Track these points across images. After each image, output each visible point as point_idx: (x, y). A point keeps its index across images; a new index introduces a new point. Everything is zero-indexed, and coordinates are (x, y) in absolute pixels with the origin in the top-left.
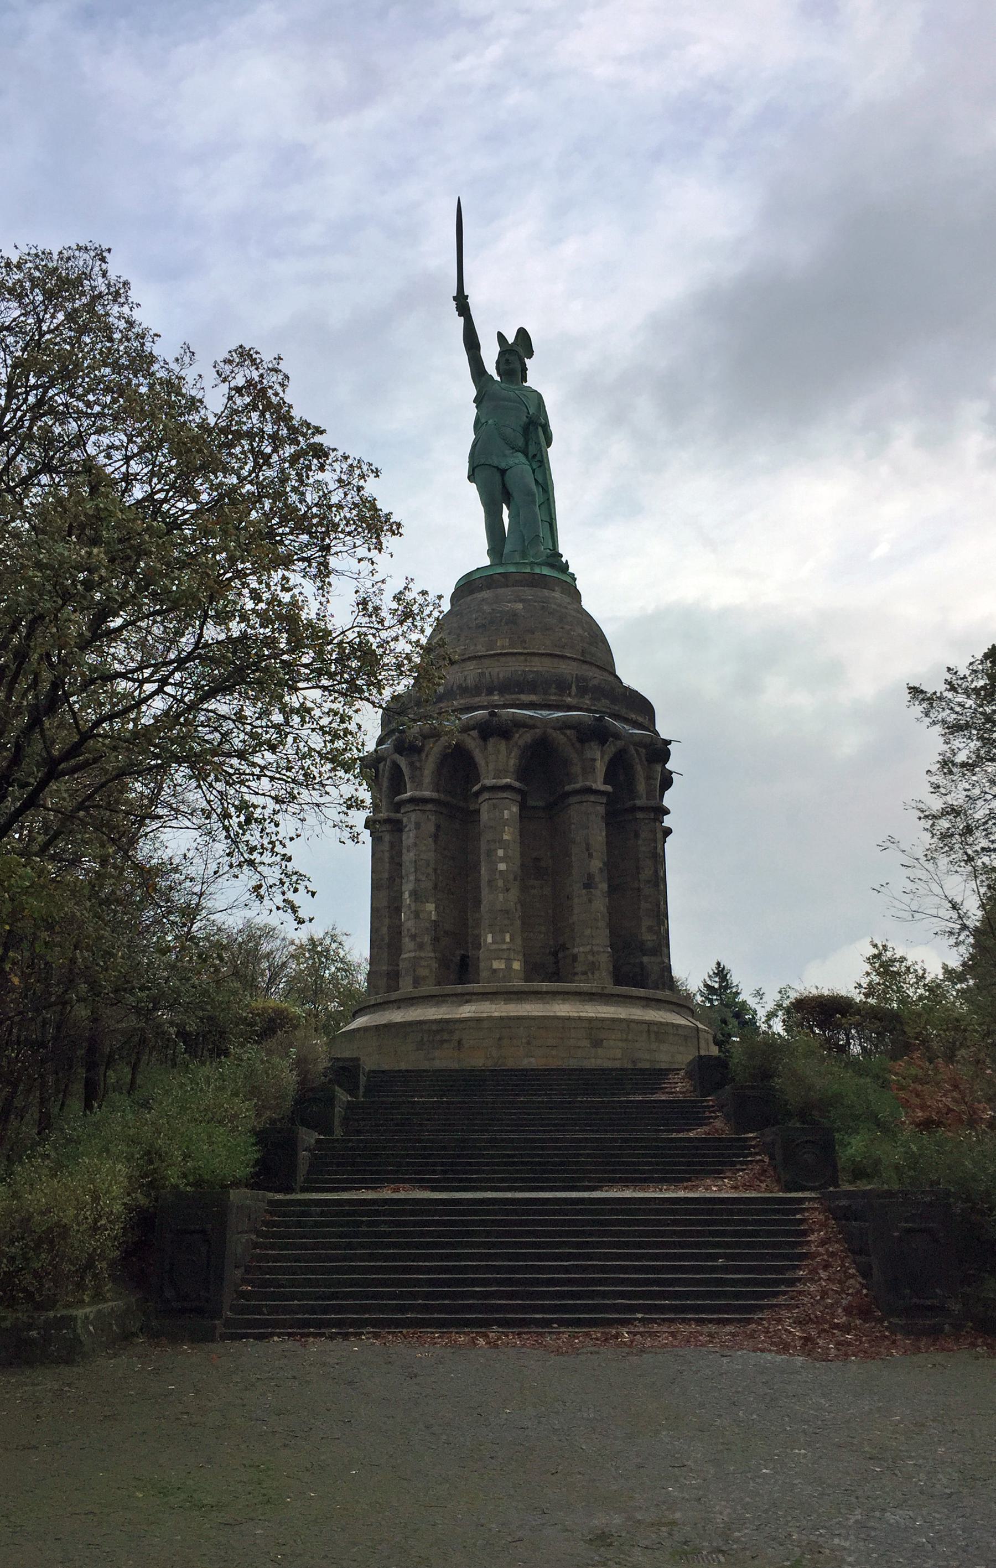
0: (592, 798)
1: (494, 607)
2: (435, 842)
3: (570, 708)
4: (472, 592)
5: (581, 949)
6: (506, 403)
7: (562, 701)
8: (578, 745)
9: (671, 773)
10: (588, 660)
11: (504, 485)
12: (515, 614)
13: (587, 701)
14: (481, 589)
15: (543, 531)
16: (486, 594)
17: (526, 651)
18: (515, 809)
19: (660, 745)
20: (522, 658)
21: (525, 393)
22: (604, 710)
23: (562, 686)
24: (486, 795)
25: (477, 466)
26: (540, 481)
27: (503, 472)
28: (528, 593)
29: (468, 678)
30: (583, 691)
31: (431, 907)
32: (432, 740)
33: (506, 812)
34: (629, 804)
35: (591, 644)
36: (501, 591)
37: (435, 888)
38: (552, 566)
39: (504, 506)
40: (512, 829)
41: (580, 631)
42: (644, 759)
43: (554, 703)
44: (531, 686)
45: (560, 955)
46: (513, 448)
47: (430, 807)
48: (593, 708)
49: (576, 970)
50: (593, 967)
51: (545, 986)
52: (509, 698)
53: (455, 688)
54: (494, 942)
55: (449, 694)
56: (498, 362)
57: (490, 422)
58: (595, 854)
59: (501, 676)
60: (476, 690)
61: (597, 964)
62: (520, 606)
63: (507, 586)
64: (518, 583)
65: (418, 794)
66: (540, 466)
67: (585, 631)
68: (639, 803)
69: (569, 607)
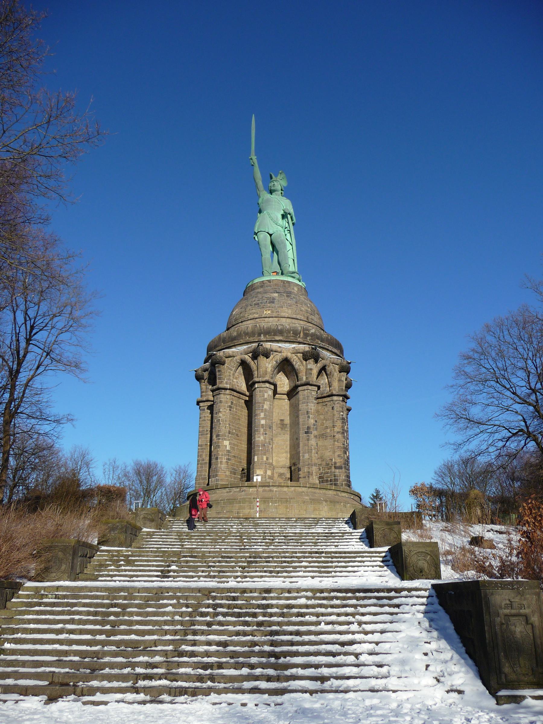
0: (310, 387)
2: (230, 410)
3: (300, 343)
8: (304, 362)
9: (351, 381)
10: (310, 321)
12: (274, 299)
14: (257, 288)
16: (260, 290)
18: (271, 393)
19: (345, 363)
20: (276, 319)
22: (317, 345)
23: (296, 333)
24: (256, 386)
27: (271, 235)
29: (249, 328)
31: (226, 443)
32: (230, 359)
33: (265, 394)
34: (330, 393)
35: (311, 314)
37: (229, 433)
40: (268, 403)
42: (337, 370)
45: (292, 469)
47: (228, 392)
48: (311, 344)
49: (300, 476)
50: (309, 474)
52: (268, 337)
53: (242, 332)
55: (239, 336)
58: (311, 416)
59: (265, 327)
60: (253, 334)
61: (311, 473)
62: (276, 295)
65: (221, 386)
68: (334, 393)
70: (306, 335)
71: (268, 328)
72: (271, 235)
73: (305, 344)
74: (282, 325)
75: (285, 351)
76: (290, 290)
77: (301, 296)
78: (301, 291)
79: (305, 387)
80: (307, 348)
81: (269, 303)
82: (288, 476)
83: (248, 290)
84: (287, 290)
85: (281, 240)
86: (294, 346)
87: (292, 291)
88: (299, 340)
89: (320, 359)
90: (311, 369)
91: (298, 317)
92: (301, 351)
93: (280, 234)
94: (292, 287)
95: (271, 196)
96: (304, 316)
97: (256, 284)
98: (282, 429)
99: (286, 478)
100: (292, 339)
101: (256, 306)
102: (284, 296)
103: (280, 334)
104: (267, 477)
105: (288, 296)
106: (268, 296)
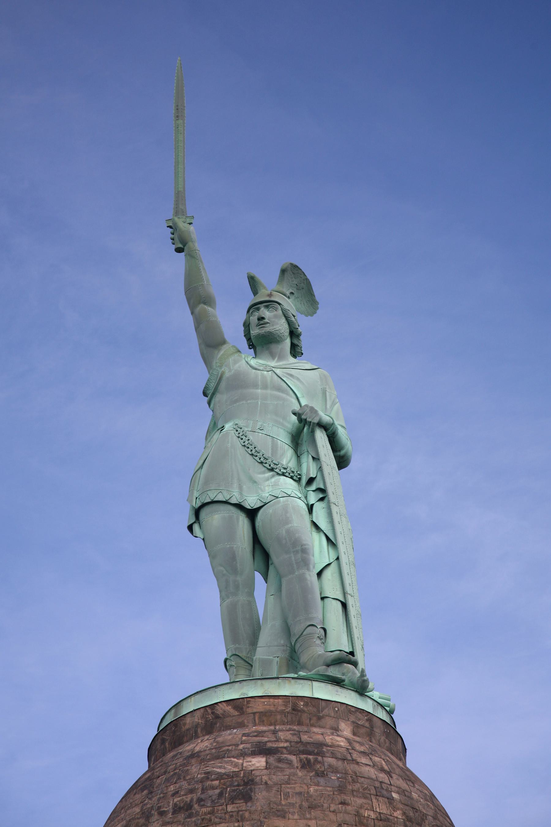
1: (209, 769)
4: (178, 742)
6: (259, 391)
11: (256, 540)
21: (293, 372)
25: (204, 505)
26: (323, 524)
36: (227, 736)
39: (258, 577)
46: (272, 470)
56: (247, 325)
57: (228, 426)
62: (259, 762)
63: (241, 725)
66: (322, 499)
67: (395, 809)
77: (364, 760)
81: (232, 800)
83: (158, 745)
84: (305, 738)
85: (288, 531)
87: (328, 739)
93: (285, 509)
94: (329, 722)
95: (253, 362)
97: (188, 720)
101: (181, 817)
105: (306, 765)
106: (230, 768)
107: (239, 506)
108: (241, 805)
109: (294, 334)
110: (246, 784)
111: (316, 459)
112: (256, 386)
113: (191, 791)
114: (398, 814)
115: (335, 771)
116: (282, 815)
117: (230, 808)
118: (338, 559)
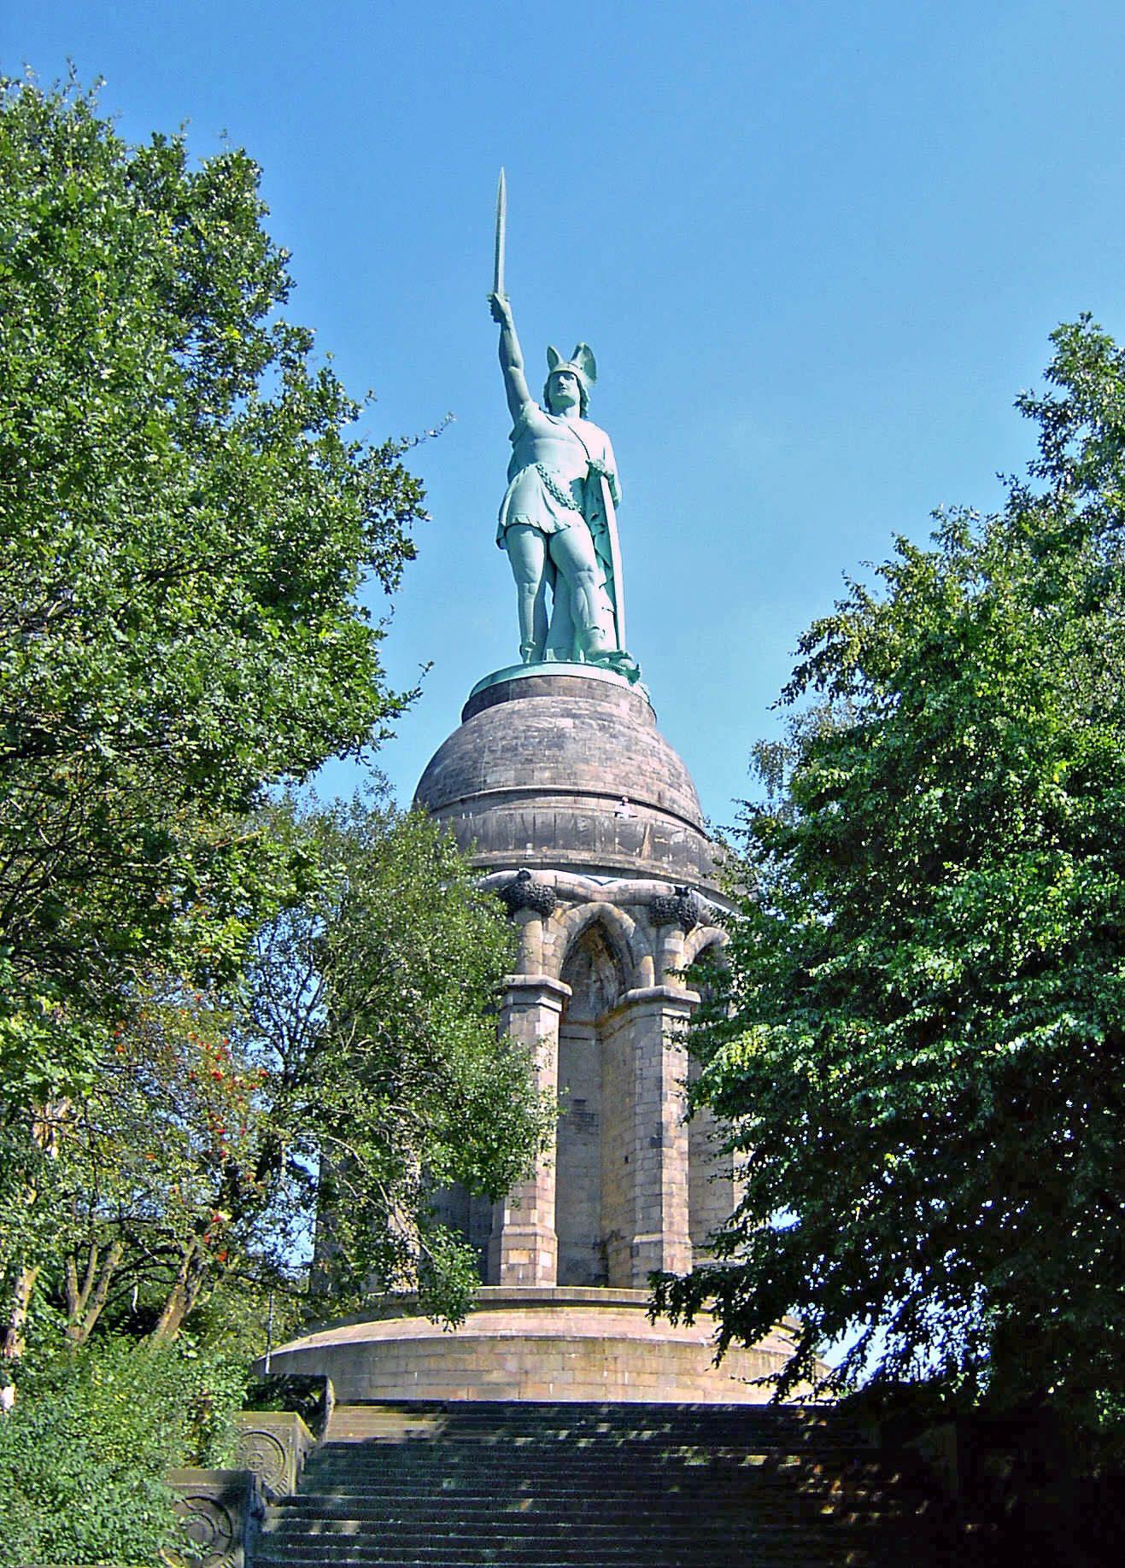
3: (640, 874)
5: (645, 1238)
7: (630, 863)
8: (652, 931)
10: (666, 805)
13: (665, 865)
15: (603, 620)
17: (576, 788)
22: (690, 880)
23: (630, 843)
27: (548, 537)
28: (583, 705)
30: (659, 850)
38: (618, 671)
39: (548, 586)
41: (658, 767)
43: (617, 865)
44: (585, 839)
45: (610, 1249)
48: (674, 876)
49: (635, 1271)
51: (590, 1293)
54: (512, 1224)
56: (547, 387)
59: (539, 821)
61: (669, 1260)
62: (567, 723)
64: (568, 691)
69: (640, 729)
70: (659, 850)
71: (550, 825)
72: (548, 537)
73: (655, 877)
74: (592, 818)
75: (597, 896)
76: (605, 707)
77: (640, 729)
78: (640, 712)
79: (654, 1007)
80: (662, 888)
82: (595, 1268)
84: (599, 709)
86: (621, 882)
87: (615, 711)
88: (640, 863)
89: (699, 924)
90: (674, 953)
91: (637, 794)
92: (649, 899)
96: (649, 790)
98: (579, 1129)
99: (590, 1275)
100: (618, 859)
101: (508, 755)
102: (591, 725)
103: (583, 844)
104: (539, 1274)
105: (602, 728)
106: (547, 725)
107: (540, 529)
108: (555, 751)
109: (583, 401)
110: (559, 737)
111: (601, 500)
112: (554, 437)
113: (516, 738)
114: (665, 772)
115: (624, 735)
116: (586, 761)
117: (547, 753)
118: (613, 579)
